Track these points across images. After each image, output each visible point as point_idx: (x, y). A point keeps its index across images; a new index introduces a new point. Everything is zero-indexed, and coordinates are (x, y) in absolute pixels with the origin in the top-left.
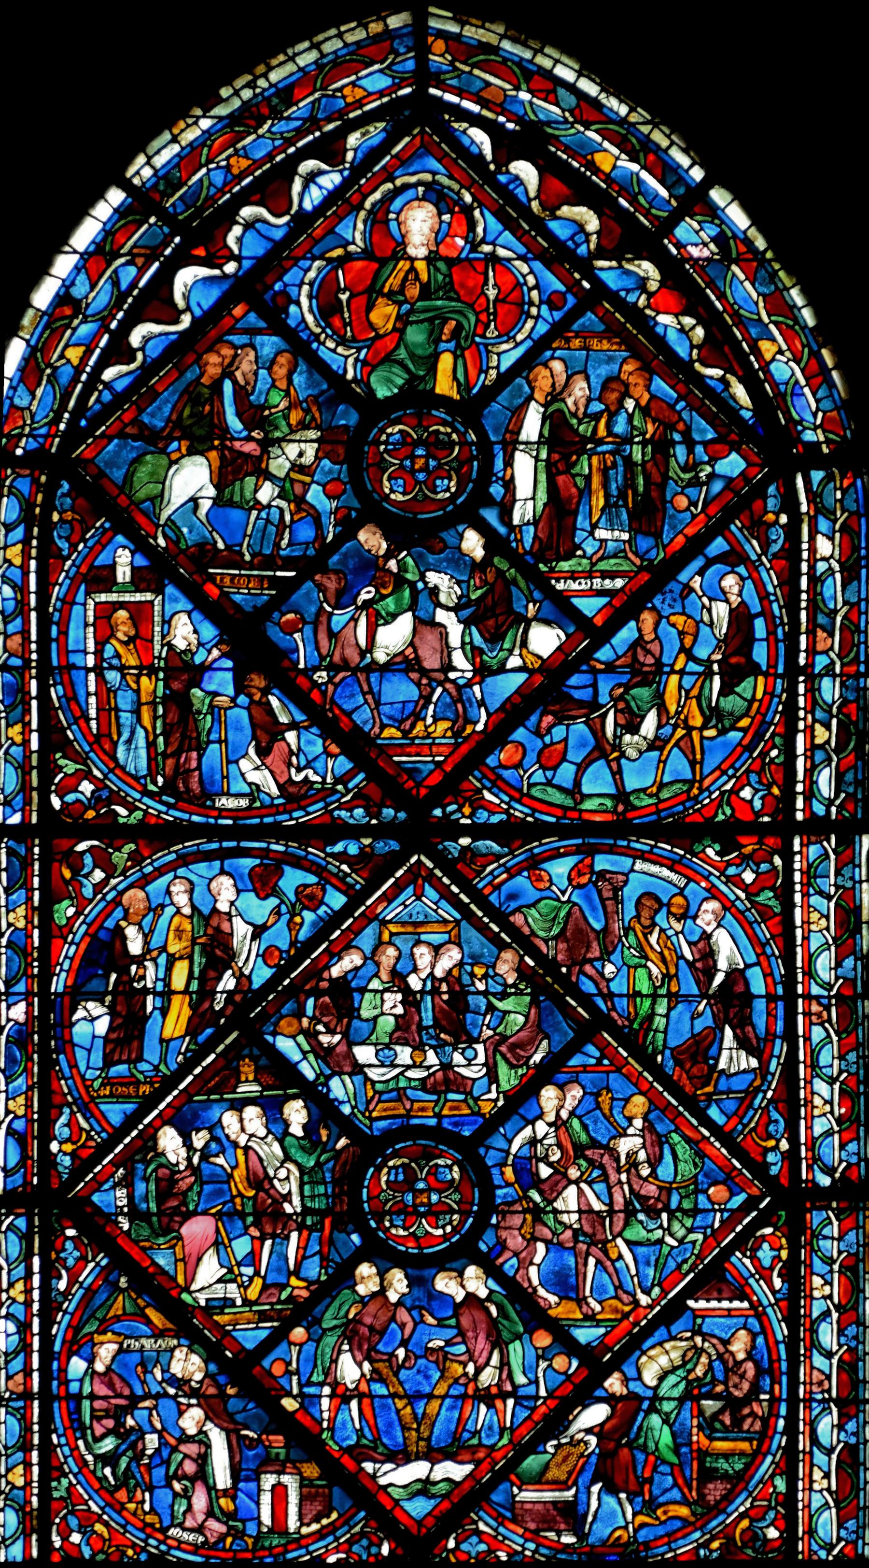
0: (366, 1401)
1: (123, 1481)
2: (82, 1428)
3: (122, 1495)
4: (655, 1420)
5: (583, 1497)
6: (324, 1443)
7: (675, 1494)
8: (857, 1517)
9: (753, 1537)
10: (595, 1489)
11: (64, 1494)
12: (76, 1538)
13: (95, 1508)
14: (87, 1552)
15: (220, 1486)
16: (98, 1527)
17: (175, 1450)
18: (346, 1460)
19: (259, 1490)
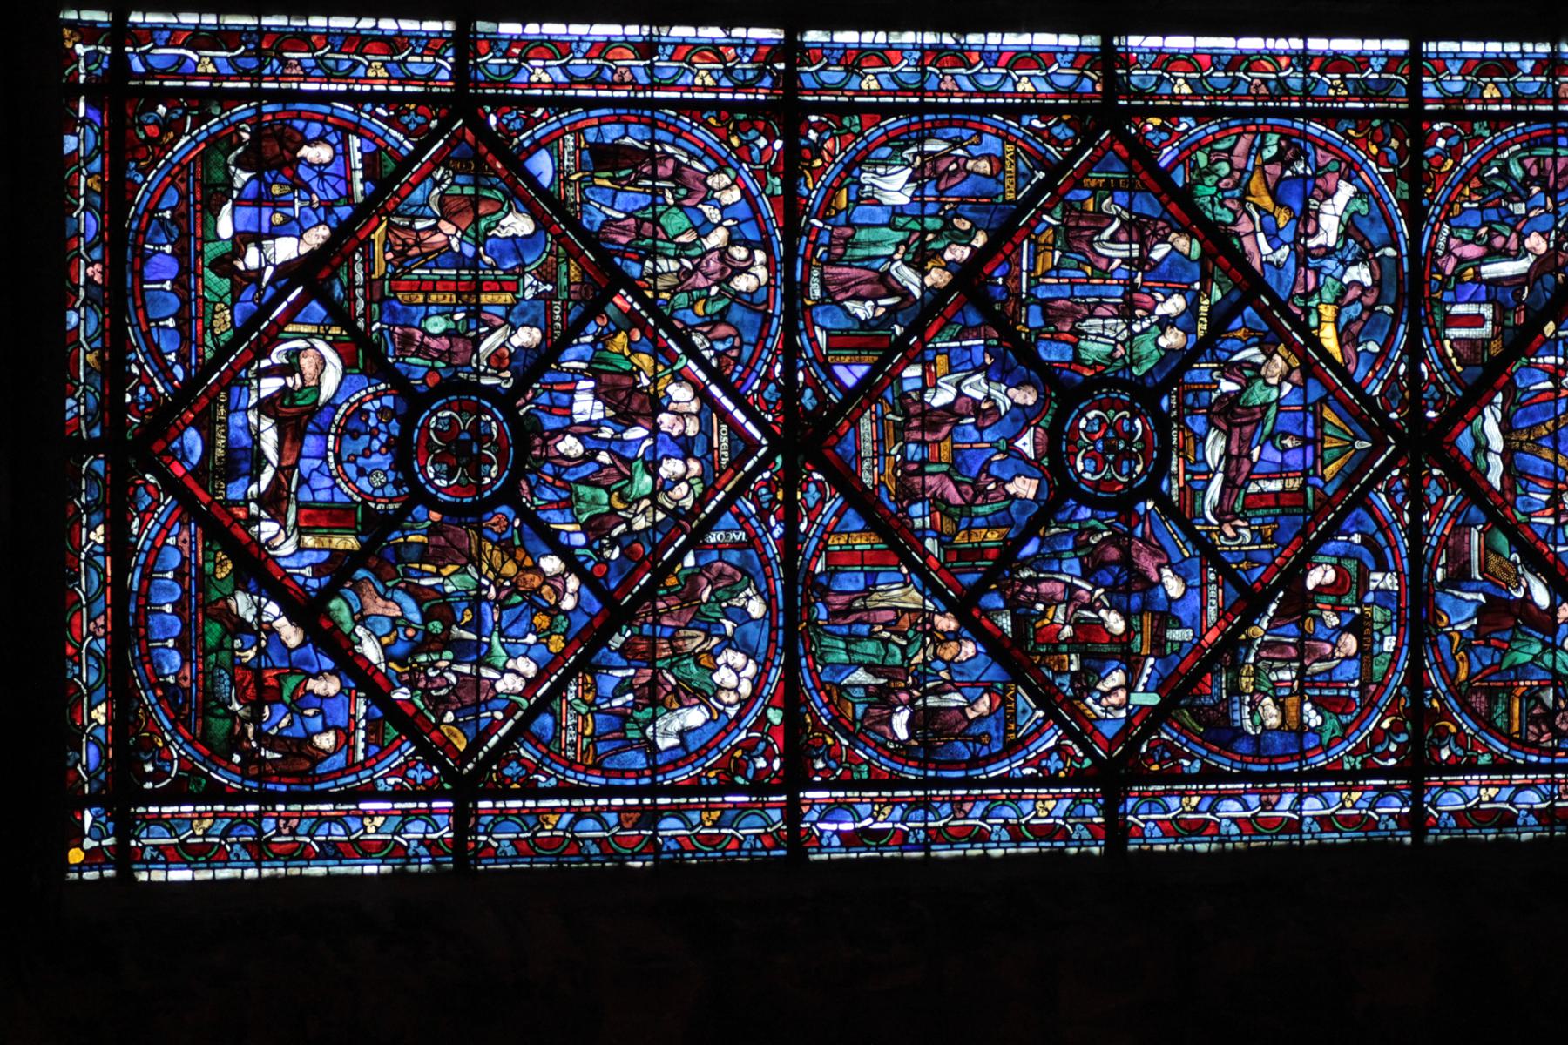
0: (1552, 395)
1: (1487, 184)
2: (1530, 148)
3: (1476, 183)
4: (1537, 648)
5: (1474, 587)
6: (1518, 359)
7: (1477, 667)
8: (1458, 827)
9: (1442, 734)
10: (1481, 597)
11: (1477, 132)
12: (1441, 143)
13: (1465, 159)
14: (1429, 153)
15: (1483, 269)
16: (1450, 163)
17: (1513, 229)
18: (1504, 378)
19: (1480, 303)
